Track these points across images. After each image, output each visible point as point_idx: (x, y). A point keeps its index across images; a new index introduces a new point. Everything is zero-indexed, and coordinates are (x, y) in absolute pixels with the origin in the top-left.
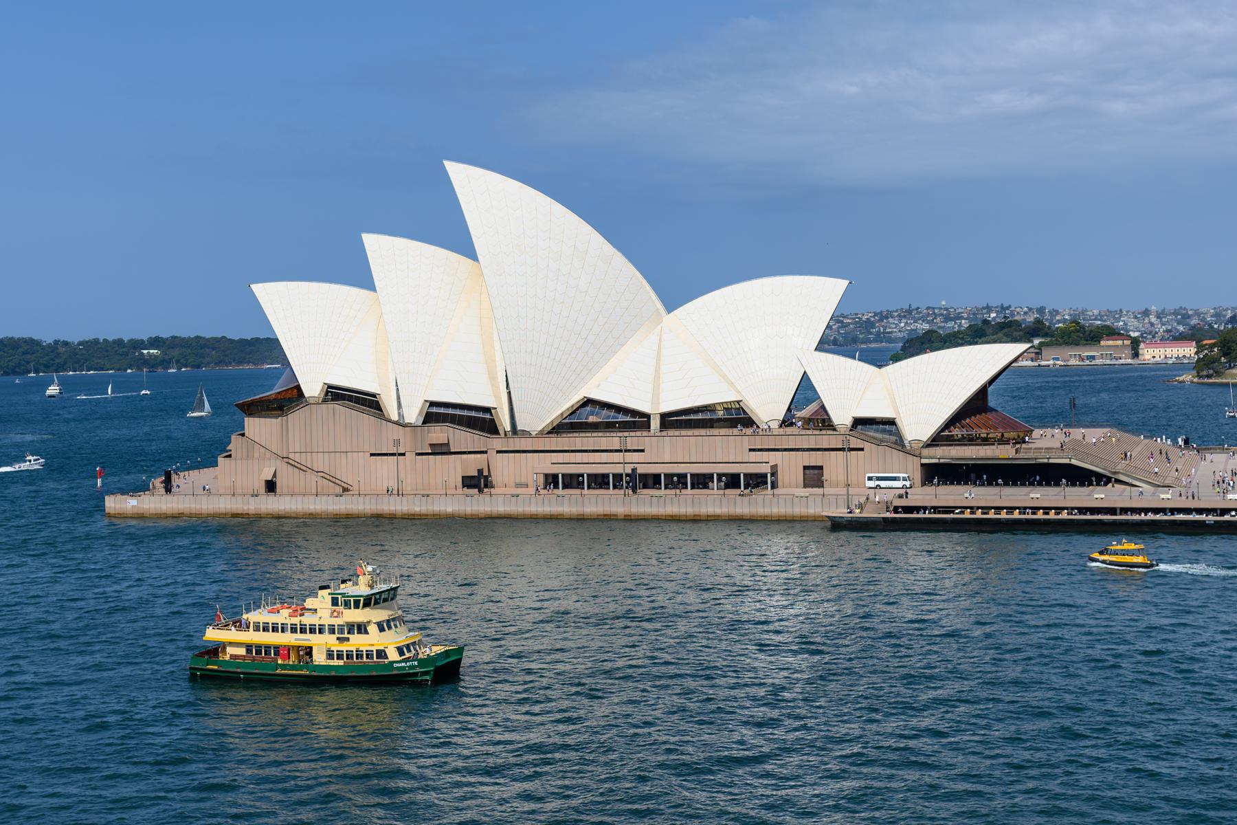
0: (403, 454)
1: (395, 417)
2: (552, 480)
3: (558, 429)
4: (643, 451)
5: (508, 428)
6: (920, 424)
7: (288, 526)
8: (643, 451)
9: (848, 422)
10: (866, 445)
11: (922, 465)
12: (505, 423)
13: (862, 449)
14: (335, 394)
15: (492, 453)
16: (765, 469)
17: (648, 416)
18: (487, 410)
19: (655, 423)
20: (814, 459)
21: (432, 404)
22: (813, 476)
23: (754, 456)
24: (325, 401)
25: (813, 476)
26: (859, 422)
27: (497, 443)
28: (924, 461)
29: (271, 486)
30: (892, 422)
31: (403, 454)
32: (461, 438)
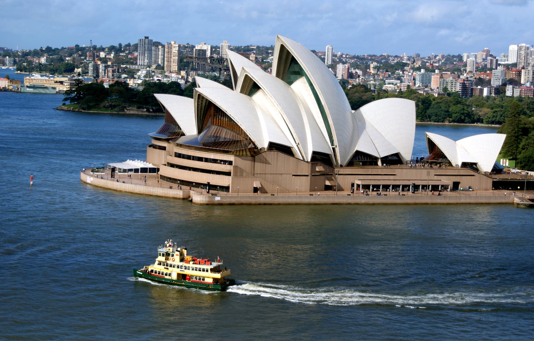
0: (307, 176)
3: (351, 164)
4: (395, 175)
6: (486, 166)
8: (395, 175)
9: (460, 164)
13: (473, 175)
14: (273, 146)
19: (379, 163)
20: (456, 179)
23: (436, 178)
25: (456, 186)
26: (464, 165)
29: (256, 190)
30: (475, 164)
31: (307, 176)
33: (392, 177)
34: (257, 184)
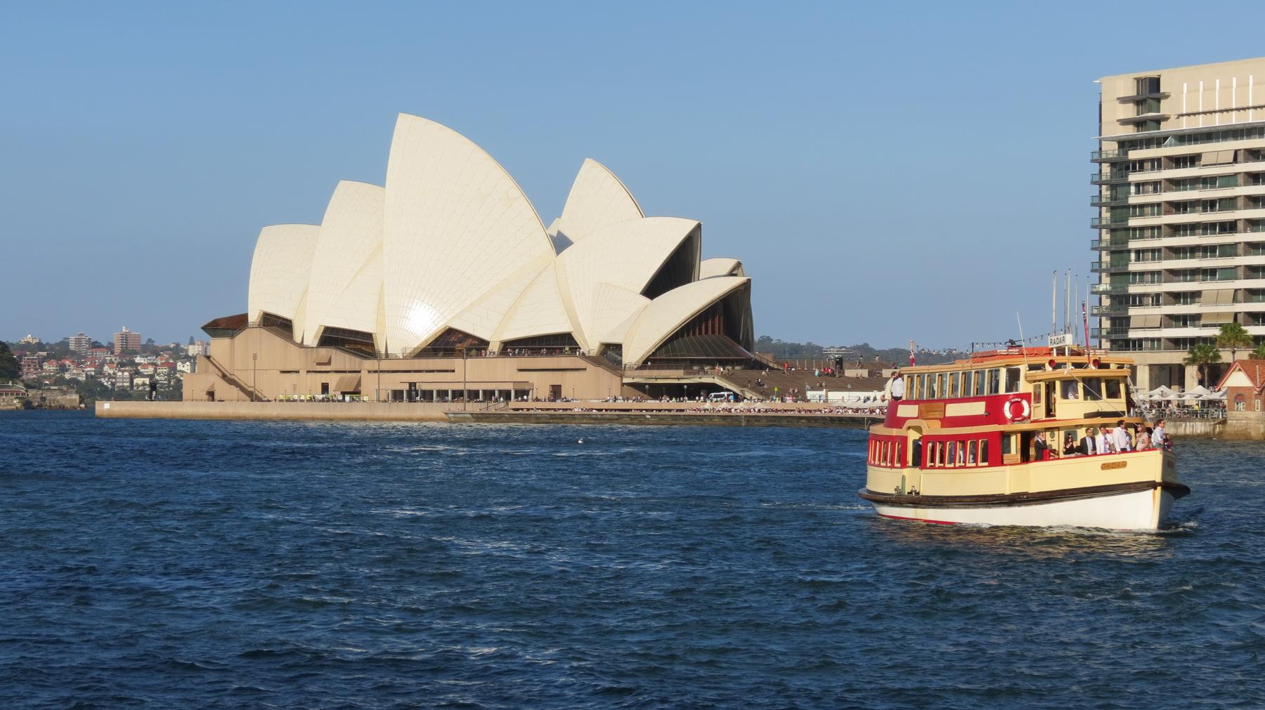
1: (298, 340)
2: (397, 395)
5: (383, 352)
7: (155, 424)
10: (590, 367)
11: (623, 384)
12: (380, 347)
15: (364, 373)
16: (510, 387)
17: (487, 343)
18: (369, 336)
21: (327, 329)
22: (556, 392)
24: (259, 326)
25: (556, 392)
27: (369, 364)
28: (625, 380)
32: (341, 359)
33: (448, 376)
34: (207, 388)
